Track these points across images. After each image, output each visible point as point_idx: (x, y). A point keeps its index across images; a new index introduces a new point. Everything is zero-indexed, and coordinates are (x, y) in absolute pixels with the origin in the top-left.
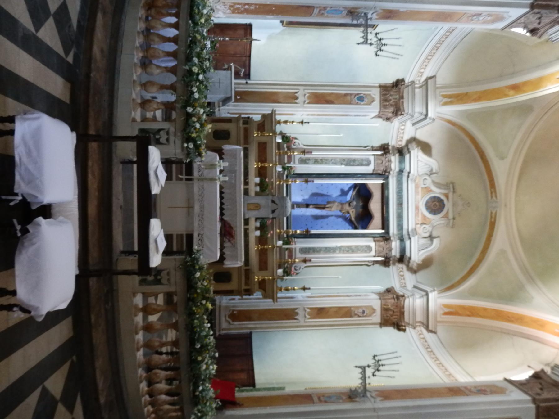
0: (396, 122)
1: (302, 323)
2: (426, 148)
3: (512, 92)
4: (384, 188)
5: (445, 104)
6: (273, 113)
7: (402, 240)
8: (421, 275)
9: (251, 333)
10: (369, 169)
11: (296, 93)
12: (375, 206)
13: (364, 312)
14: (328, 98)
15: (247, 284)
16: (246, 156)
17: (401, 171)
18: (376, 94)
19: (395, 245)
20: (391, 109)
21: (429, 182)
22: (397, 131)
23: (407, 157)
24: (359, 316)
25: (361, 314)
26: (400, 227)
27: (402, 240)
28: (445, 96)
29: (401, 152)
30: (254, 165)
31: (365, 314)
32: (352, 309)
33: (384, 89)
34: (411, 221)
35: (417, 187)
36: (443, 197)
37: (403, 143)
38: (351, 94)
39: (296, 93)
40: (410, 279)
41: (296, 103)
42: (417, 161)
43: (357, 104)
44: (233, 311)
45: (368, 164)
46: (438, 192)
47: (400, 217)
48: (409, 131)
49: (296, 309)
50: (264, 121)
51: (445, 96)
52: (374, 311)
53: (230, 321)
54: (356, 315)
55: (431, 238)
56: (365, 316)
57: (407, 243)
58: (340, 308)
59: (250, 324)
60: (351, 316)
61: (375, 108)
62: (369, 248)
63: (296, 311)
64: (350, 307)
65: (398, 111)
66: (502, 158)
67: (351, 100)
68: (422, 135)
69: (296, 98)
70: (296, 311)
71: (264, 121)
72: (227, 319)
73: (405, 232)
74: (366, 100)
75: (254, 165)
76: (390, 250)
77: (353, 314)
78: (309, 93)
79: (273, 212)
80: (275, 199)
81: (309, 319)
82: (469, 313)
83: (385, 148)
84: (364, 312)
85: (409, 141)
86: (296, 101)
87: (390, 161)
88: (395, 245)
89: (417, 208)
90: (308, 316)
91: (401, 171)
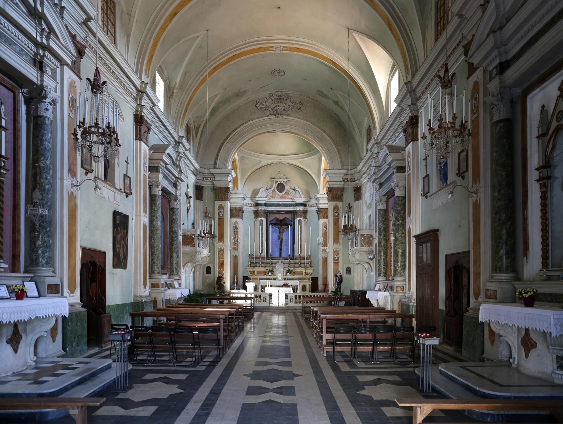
0: (245, 208)
2: (255, 192)
4: (272, 212)
5: (237, 188)
7: (296, 205)
8: (312, 196)
10: (264, 220)
12: (281, 217)
17: (266, 205)
18: (234, 220)
19: (298, 208)
20: (240, 213)
21: (270, 191)
22: (249, 210)
23: (259, 202)
26: (290, 205)
27: (296, 205)
28: (234, 189)
29: (257, 205)
33: (232, 216)
34: (288, 201)
35: (272, 197)
37: (253, 203)
40: (313, 201)
42: (261, 198)
45: (262, 221)
46: (275, 186)
47: (286, 205)
48: (248, 201)
51: (234, 189)
52: (325, 222)
55: (294, 190)
57: (297, 202)
61: (239, 220)
62: (300, 221)
65: (241, 210)
68: (249, 195)
73: (293, 203)
76: (300, 210)
83: (257, 214)
85: (252, 201)
87: (261, 210)
88: (298, 208)
89: (282, 197)
91: (266, 205)
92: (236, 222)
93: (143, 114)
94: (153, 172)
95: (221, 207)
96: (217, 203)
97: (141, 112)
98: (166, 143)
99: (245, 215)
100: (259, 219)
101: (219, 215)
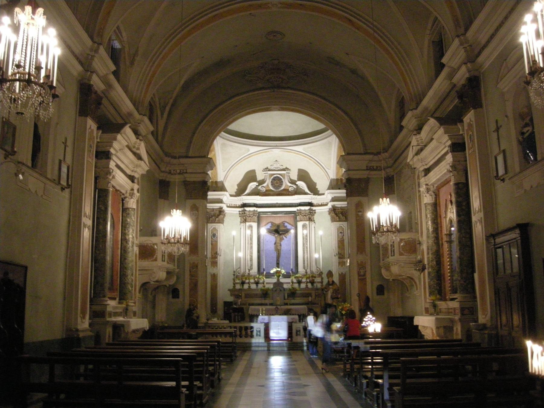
6: (229, 290)
13: (341, 233)
16: (253, 305)
24: (344, 235)
30: (258, 301)
36: (272, 178)
38: (212, 241)
43: (217, 238)
60: (343, 240)
66: (249, 150)
69: (214, 274)
74: (214, 232)
75: (258, 301)
79: (281, 290)
80: (274, 289)
84: (341, 233)
92: (214, 228)
93: (92, 83)
94: (102, 158)
97: (89, 79)
98: (120, 121)
99: (226, 219)
100: (248, 224)
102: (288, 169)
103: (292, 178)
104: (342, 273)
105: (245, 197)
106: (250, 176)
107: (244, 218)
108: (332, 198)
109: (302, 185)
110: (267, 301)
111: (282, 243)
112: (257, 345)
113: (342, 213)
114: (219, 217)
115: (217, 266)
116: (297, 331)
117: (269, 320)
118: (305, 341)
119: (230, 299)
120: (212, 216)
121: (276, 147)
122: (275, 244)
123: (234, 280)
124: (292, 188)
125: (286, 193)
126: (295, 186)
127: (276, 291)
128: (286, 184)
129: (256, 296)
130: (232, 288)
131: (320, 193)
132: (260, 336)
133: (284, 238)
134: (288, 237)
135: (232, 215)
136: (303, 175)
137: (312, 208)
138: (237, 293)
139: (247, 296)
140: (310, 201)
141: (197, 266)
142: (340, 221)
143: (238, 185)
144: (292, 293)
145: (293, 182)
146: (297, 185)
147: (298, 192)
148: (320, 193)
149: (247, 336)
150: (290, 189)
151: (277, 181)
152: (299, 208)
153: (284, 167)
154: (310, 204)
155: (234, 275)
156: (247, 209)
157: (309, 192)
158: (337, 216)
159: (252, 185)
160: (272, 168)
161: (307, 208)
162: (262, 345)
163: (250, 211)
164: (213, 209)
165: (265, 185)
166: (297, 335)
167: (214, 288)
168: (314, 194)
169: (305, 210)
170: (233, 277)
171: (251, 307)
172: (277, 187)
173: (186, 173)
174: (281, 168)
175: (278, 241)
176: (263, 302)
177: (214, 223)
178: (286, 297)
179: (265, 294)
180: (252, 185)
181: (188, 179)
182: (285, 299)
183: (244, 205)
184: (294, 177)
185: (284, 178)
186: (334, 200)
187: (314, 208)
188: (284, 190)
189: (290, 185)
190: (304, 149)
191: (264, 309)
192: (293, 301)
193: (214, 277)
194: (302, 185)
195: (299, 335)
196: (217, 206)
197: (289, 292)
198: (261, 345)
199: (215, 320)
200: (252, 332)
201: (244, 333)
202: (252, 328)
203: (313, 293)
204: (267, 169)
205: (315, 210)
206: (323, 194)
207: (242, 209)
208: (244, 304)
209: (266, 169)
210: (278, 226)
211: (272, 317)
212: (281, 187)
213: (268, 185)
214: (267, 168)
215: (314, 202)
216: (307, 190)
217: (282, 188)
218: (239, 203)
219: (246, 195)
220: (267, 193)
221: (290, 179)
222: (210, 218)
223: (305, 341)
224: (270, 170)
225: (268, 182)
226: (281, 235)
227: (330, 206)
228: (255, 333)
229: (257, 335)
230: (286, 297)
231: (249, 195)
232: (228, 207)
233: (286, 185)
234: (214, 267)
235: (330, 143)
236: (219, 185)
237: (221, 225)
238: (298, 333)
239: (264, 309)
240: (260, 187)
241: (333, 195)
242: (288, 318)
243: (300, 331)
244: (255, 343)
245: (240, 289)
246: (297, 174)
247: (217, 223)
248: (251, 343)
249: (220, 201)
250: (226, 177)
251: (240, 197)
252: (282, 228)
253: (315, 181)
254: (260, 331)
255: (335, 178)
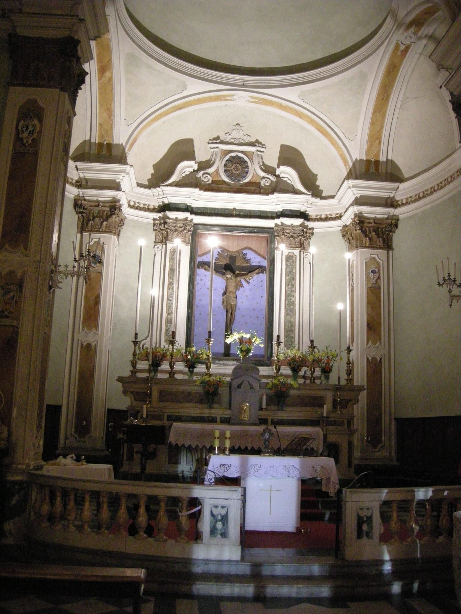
1: (386, 352)
3: (107, 74)
6: (120, 379)
9: (396, 419)
11: (82, 345)
13: (373, 272)
14: (92, 302)
15: (341, 424)
16: (179, 419)
24: (379, 278)
25: (377, 276)
30: (194, 410)
31: (377, 270)
32: (369, 286)
36: (227, 157)
39: (82, 345)
41: (96, 345)
44: (367, 441)
49: (368, 359)
50: (132, 393)
53: (380, 446)
54: (376, 281)
56: (379, 270)
58: (369, 302)
59: (385, 420)
60: (379, 288)
63: (370, 358)
64: (368, 288)
67: (97, 272)
69: (89, 345)
70: (370, 358)
71: (132, 393)
72: (377, 450)
75: (194, 410)
77: (376, 286)
78: (83, 327)
80: (235, 383)
81: (381, 343)
82: (377, 141)
84: (373, 272)
86: (93, 345)
90: (378, 344)
92: (98, 243)
95: (31, 112)
96: (18, 96)
99: (125, 231)
101: (18, 139)
102: (260, 143)
103: (268, 163)
104: (374, 358)
105: (169, 188)
106: (183, 150)
107: (163, 233)
108: (356, 199)
109: (288, 174)
110: (217, 412)
111: (238, 293)
112: (213, 568)
113: (376, 231)
114: (110, 220)
115: (97, 328)
116: (360, 521)
117: (244, 468)
118: (387, 557)
119: (123, 403)
120: (94, 218)
121: (243, 87)
122: (225, 293)
123: (134, 365)
124: (267, 180)
125: (254, 188)
126: (273, 178)
127: (239, 386)
128: (255, 172)
129: (188, 397)
130: (126, 373)
131: (324, 194)
132: (224, 535)
133: (243, 281)
134: (251, 281)
135: (137, 225)
136: (290, 156)
137: (307, 223)
138: (138, 388)
139: (164, 396)
140: (303, 209)
141: (20, 285)
142: (371, 247)
143: (155, 166)
144: (279, 396)
145: (268, 169)
146: (278, 177)
147: (280, 187)
148: (324, 194)
149: (175, 532)
150: (263, 183)
151: (237, 165)
152: (278, 221)
153: (253, 140)
154: (303, 215)
155: (135, 343)
156: (172, 215)
157: (303, 189)
158: (366, 236)
159: (186, 167)
160: (228, 138)
161: (297, 222)
162: (234, 570)
163: (176, 219)
164: (98, 202)
165: (211, 170)
166: (359, 536)
167: (86, 377)
168: (313, 195)
169: (292, 226)
170: (131, 357)
171: (175, 424)
172: (237, 175)
173: (20, 11)
174: (247, 140)
175: (231, 288)
176: (206, 412)
177: (98, 231)
178: (264, 406)
179: (211, 392)
180: (186, 167)
181: (21, 32)
182: (261, 409)
183: (165, 207)
184: (272, 160)
185: (252, 161)
186: (359, 201)
187: (310, 224)
188: (249, 183)
189: (262, 174)
190: (301, 96)
191: (228, 435)
192: (283, 415)
193: (89, 352)
194: (288, 174)
195: (369, 535)
196: (106, 195)
197: (271, 392)
198: (225, 569)
199: (66, 467)
200: (196, 517)
201: (163, 519)
202: (195, 502)
203: (329, 396)
204: (216, 140)
205: (312, 229)
206: (333, 197)
207: (161, 215)
208: (160, 417)
209: (214, 139)
210: (233, 258)
211: (254, 460)
212: (244, 177)
213: (217, 171)
214: (218, 138)
215: (312, 212)
216: (299, 186)
217: (247, 180)
218: (156, 203)
219: (171, 185)
220: (215, 187)
221: (264, 164)
222: (89, 220)
223: (387, 557)
224: (222, 142)
225: (219, 166)
226: (237, 276)
227: (348, 219)
228: (205, 524)
229: (213, 531)
230: (264, 406)
231: (177, 184)
232: (130, 206)
233: (255, 175)
234: (90, 328)
235: (363, 77)
236: (115, 152)
237: (114, 238)
238: (365, 527)
239: (228, 435)
240: (200, 174)
241: (358, 193)
242: (302, 465)
243: (369, 519)
244: (207, 561)
245: (146, 380)
246: (278, 155)
247: (105, 232)
248: (188, 562)
249: (116, 186)
250: (133, 140)
251: (158, 189)
252: (239, 263)
253: (315, 172)
254: (225, 519)
255: (364, 158)
